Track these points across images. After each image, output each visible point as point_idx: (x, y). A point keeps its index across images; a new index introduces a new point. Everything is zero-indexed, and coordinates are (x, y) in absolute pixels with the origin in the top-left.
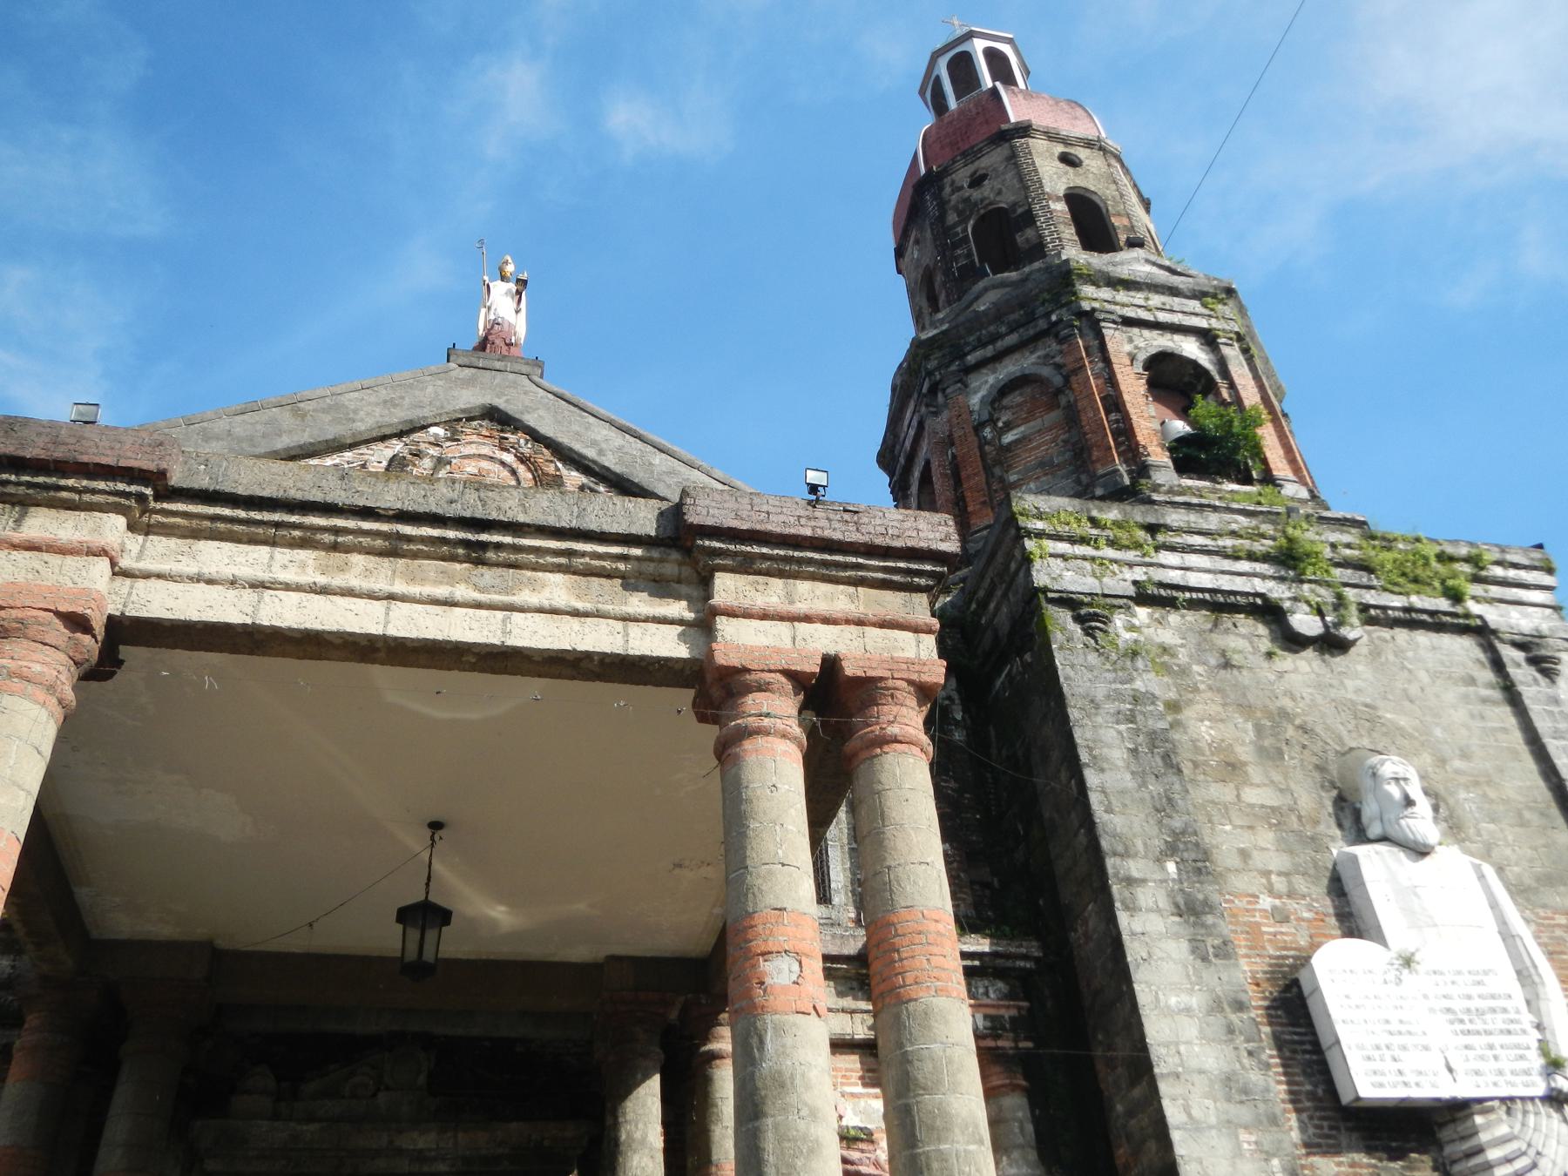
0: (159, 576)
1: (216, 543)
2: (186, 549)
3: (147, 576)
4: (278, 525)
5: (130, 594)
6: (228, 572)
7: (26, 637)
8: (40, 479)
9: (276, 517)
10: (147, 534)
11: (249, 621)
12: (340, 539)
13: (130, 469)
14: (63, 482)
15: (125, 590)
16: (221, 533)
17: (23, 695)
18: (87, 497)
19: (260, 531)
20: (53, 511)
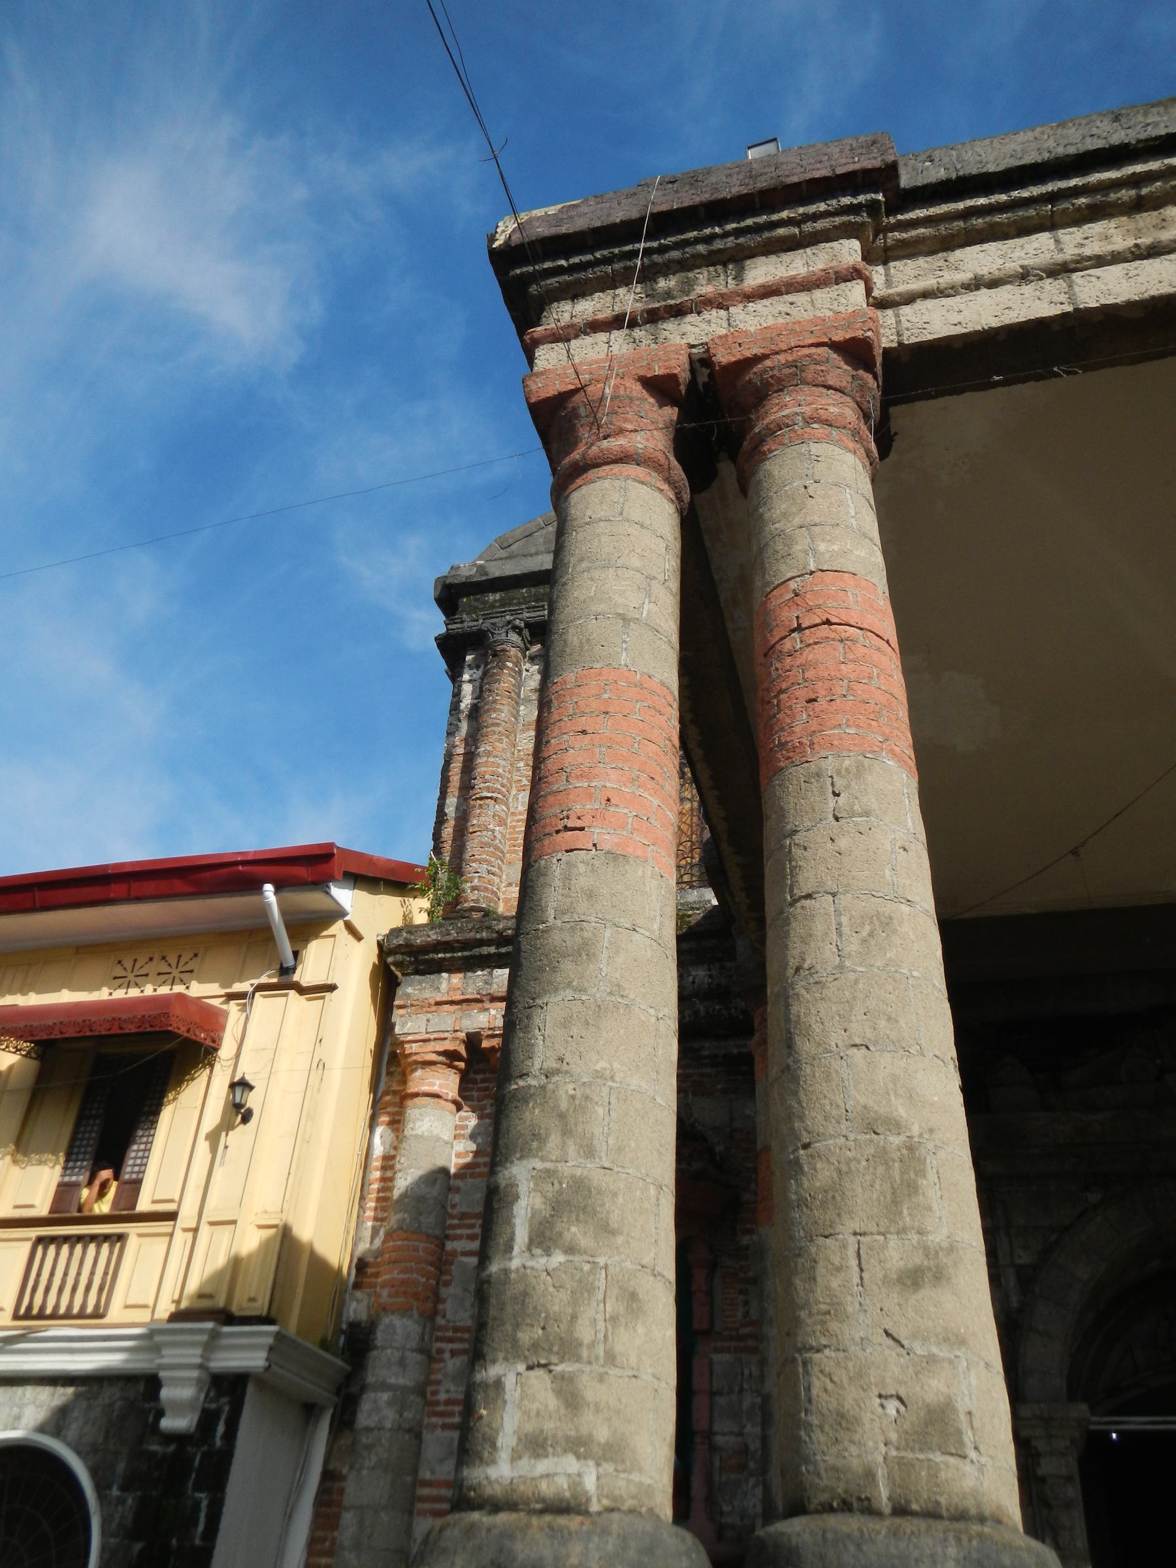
0: (926, 295)
1: (977, 248)
2: (941, 263)
3: (910, 299)
4: (1052, 198)
5: (898, 322)
6: (1013, 266)
7: (804, 382)
8: (749, 222)
9: (1050, 187)
10: (885, 263)
11: (1070, 309)
12: (1144, 191)
13: (852, 175)
14: (775, 217)
15: (893, 320)
16: (979, 231)
17: (828, 440)
18: (808, 227)
19: (1032, 212)
20: (773, 258)
